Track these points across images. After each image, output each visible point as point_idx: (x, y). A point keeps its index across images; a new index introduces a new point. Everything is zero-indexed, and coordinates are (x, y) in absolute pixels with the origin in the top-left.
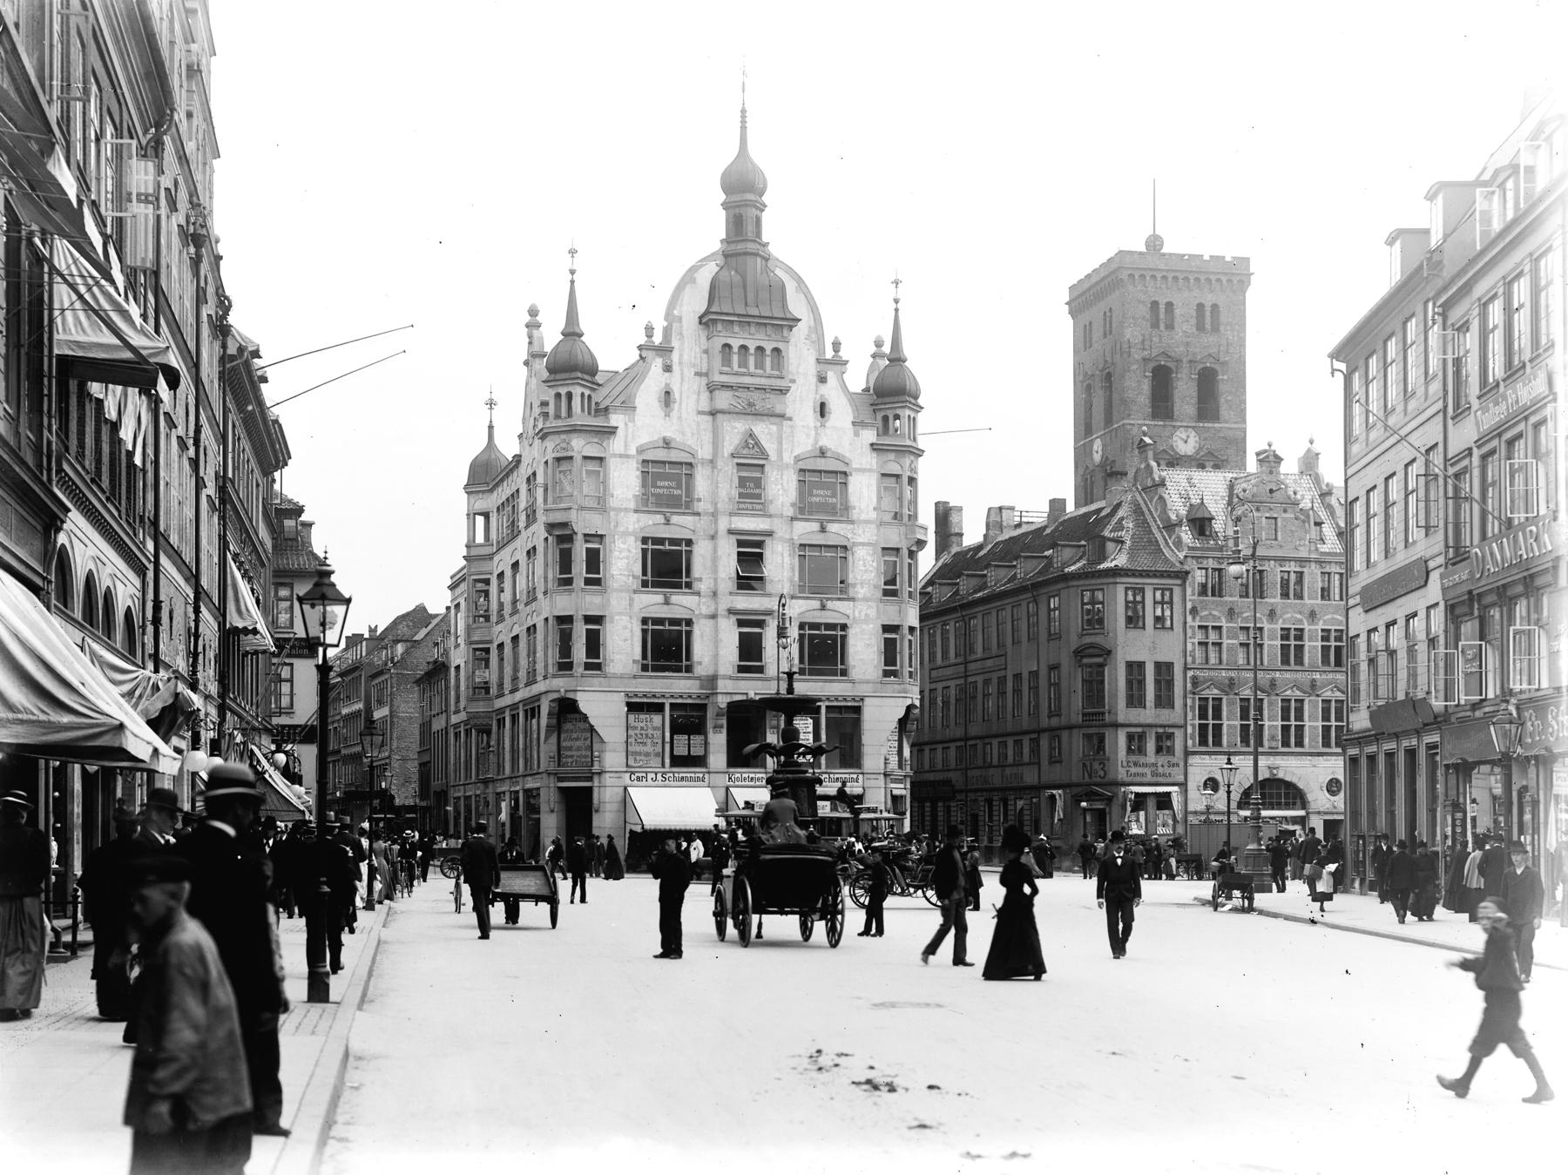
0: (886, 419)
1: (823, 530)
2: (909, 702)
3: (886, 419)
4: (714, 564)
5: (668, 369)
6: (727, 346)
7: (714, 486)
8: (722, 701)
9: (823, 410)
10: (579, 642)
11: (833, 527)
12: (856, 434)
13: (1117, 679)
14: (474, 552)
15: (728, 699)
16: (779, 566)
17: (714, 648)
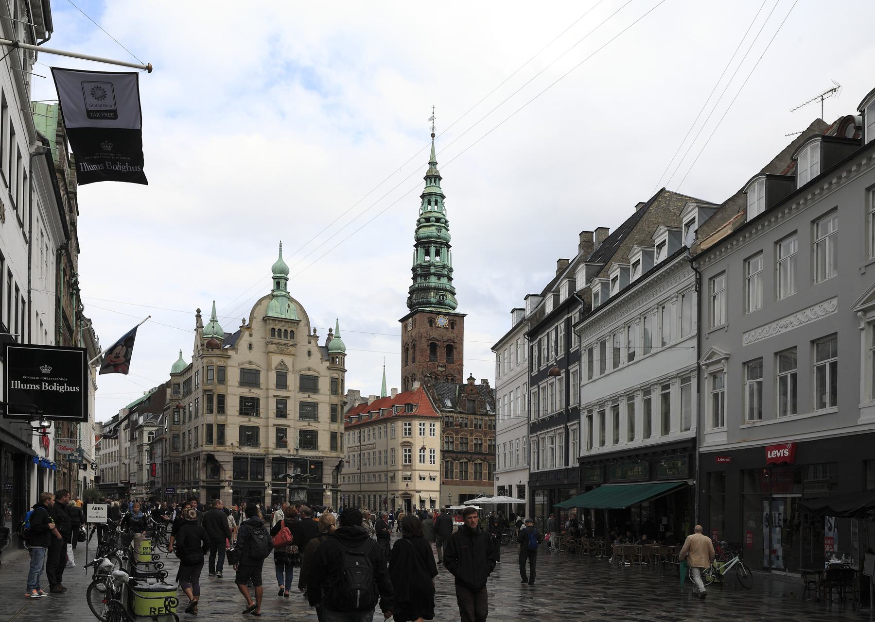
1: (309, 396)
4: (268, 407)
7: (269, 379)
8: (271, 457)
10: (218, 434)
11: (312, 396)
13: (416, 454)
15: (273, 456)
16: (293, 408)
17: (267, 438)
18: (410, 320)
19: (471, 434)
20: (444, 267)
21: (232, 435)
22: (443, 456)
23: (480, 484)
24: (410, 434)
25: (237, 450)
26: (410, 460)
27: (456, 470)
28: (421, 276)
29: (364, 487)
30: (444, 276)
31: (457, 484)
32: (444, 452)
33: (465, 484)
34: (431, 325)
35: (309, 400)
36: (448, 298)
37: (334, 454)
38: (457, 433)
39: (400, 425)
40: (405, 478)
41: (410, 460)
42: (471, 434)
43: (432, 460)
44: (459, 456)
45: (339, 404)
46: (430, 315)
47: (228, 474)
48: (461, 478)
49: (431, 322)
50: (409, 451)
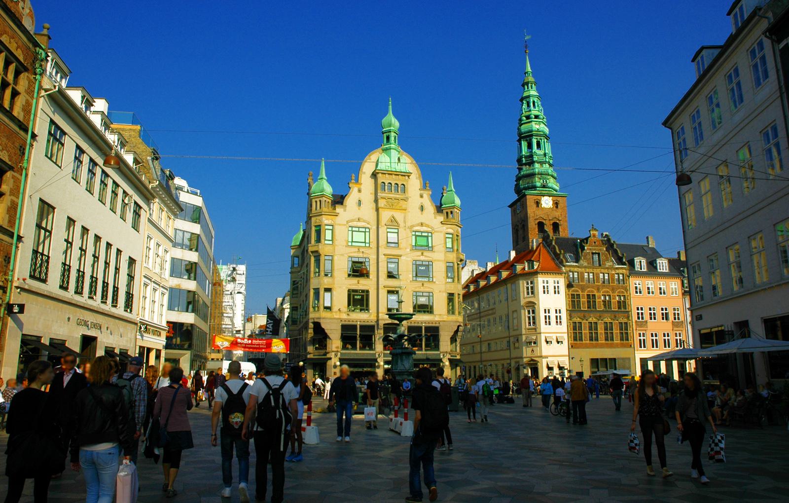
0: (447, 213)
2: (458, 324)
3: (447, 213)
5: (360, 191)
6: (383, 182)
8: (381, 323)
9: (422, 208)
11: (426, 253)
12: (435, 218)
14: (294, 270)
18: (519, 204)
19: (598, 290)
20: (545, 155)
21: (339, 299)
22: (570, 316)
23: (611, 346)
24: (532, 293)
25: (344, 316)
26: (534, 323)
27: (586, 331)
28: (525, 164)
29: (486, 356)
30: (545, 162)
31: (586, 346)
32: (570, 313)
33: (596, 346)
34: (538, 206)
35: (422, 258)
36: (552, 183)
37: (452, 318)
38: (583, 290)
39: (523, 284)
40: (530, 343)
41: (534, 323)
42: (598, 290)
43: (559, 321)
44: (586, 314)
45: (455, 260)
46: (536, 197)
47: (335, 343)
48: (591, 339)
49: (538, 203)
50: (533, 312)
